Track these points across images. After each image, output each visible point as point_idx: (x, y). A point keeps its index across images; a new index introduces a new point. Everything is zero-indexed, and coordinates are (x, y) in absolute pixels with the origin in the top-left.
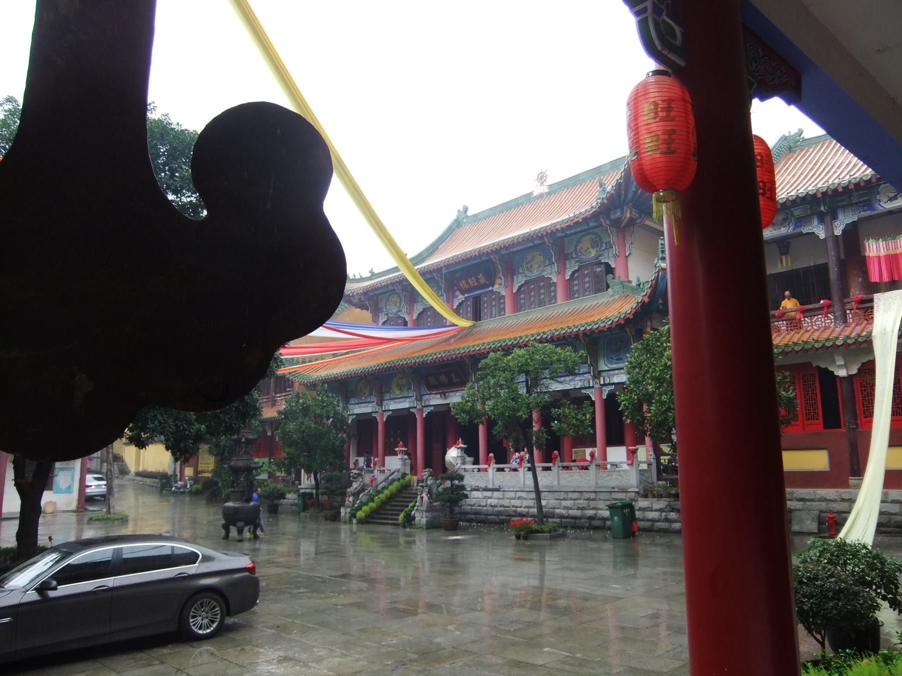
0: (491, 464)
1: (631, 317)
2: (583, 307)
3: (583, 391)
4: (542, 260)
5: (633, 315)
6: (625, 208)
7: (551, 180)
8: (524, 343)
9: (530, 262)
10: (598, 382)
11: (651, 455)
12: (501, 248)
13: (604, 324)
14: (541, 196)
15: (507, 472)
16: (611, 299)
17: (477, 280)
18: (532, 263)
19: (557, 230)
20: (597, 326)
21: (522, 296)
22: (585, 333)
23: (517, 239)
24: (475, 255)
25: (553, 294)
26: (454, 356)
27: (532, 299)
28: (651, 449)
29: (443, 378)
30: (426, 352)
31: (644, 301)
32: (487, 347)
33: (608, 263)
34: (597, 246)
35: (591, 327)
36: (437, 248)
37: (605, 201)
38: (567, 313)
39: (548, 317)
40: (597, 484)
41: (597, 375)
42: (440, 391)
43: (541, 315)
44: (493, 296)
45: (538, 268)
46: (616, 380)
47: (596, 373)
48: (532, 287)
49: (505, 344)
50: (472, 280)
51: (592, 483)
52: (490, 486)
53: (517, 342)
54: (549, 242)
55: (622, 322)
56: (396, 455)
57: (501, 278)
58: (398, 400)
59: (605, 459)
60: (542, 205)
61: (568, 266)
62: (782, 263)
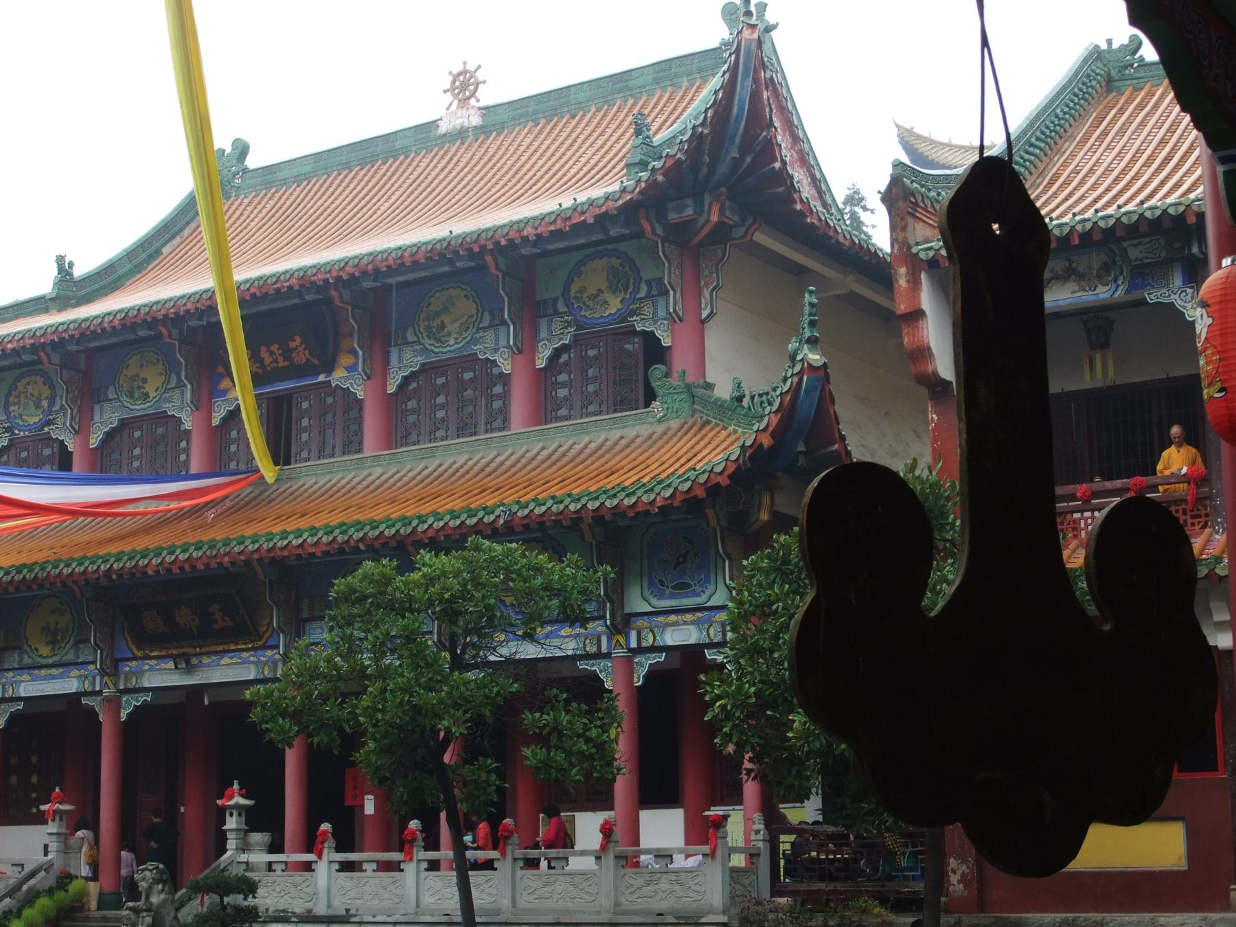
0: (325, 851)
1: (724, 481)
2: (583, 444)
3: (583, 665)
4: (474, 312)
5: (730, 476)
6: (707, 199)
7: (489, 96)
8: (430, 534)
9: (438, 314)
10: (622, 641)
11: (757, 832)
12: (364, 273)
13: (652, 497)
14: (460, 134)
15: (370, 873)
16: (660, 429)
17: (287, 353)
18: (446, 319)
19: (525, 239)
20: (633, 500)
21: (411, 404)
22: (598, 517)
23: (412, 255)
24: (290, 288)
25: (497, 404)
26: (226, 559)
27: (440, 414)
28: (757, 816)
29: (185, 617)
30: (140, 544)
31: (761, 444)
32: (324, 540)
33: (653, 332)
34: (626, 289)
35: (615, 502)
36: (158, 252)
37: (660, 178)
38: (540, 458)
39: (487, 465)
40: (617, 904)
41: (622, 624)
42: (175, 652)
43: (466, 457)
44: (330, 400)
45: (460, 333)
46: (671, 638)
47: (619, 619)
48: (441, 381)
49: (377, 533)
50: (271, 353)
51: (606, 902)
52: (321, 909)
53: (409, 530)
54: (497, 268)
55: (700, 493)
56: (44, 822)
57: (355, 354)
58: (44, 672)
59: (636, 842)
60: (465, 160)
61: (543, 334)
62: (1092, 368)
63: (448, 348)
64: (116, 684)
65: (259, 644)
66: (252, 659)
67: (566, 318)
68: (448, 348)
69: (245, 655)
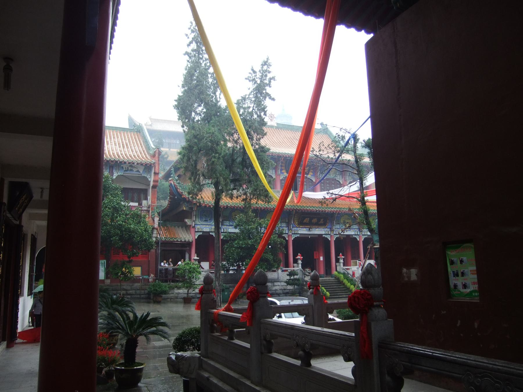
64: (292, 232)
69: (321, 229)
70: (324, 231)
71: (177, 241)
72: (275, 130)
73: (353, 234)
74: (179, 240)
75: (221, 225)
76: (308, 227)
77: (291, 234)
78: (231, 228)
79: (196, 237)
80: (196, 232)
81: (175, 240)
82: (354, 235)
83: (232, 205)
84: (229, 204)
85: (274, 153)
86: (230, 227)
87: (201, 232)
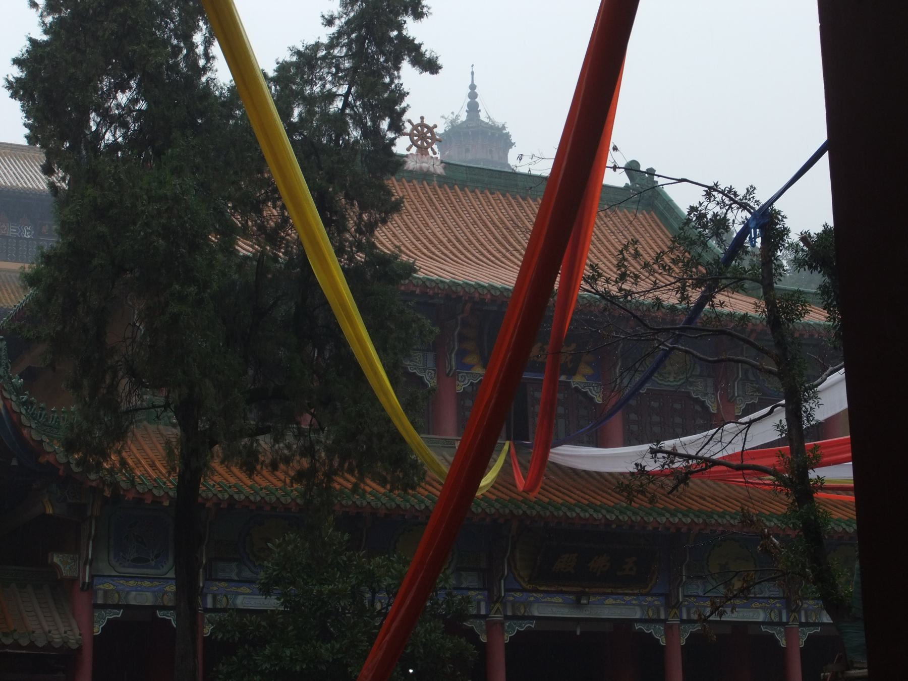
63: (669, 383)
65: (644, 591)
66: (634, 602)
67: (755, 385)
68: (669, 383)
69: (627, 598)
70: (640, 606)
71: (16, 645)
72: (436, 193)
73: (760, 620)
74: (24, 642)
75: (206, 580)
76: (575, 589)
77: (499, 617)
78: (248, 591)
79: (98, 630)
80: (97, 606)
81: (8, 641)
82: (763, 623)
83: (252, 498)
84: (240, 492)
85: (434, 285)
86: (245, 589)
87: (117, 607)
